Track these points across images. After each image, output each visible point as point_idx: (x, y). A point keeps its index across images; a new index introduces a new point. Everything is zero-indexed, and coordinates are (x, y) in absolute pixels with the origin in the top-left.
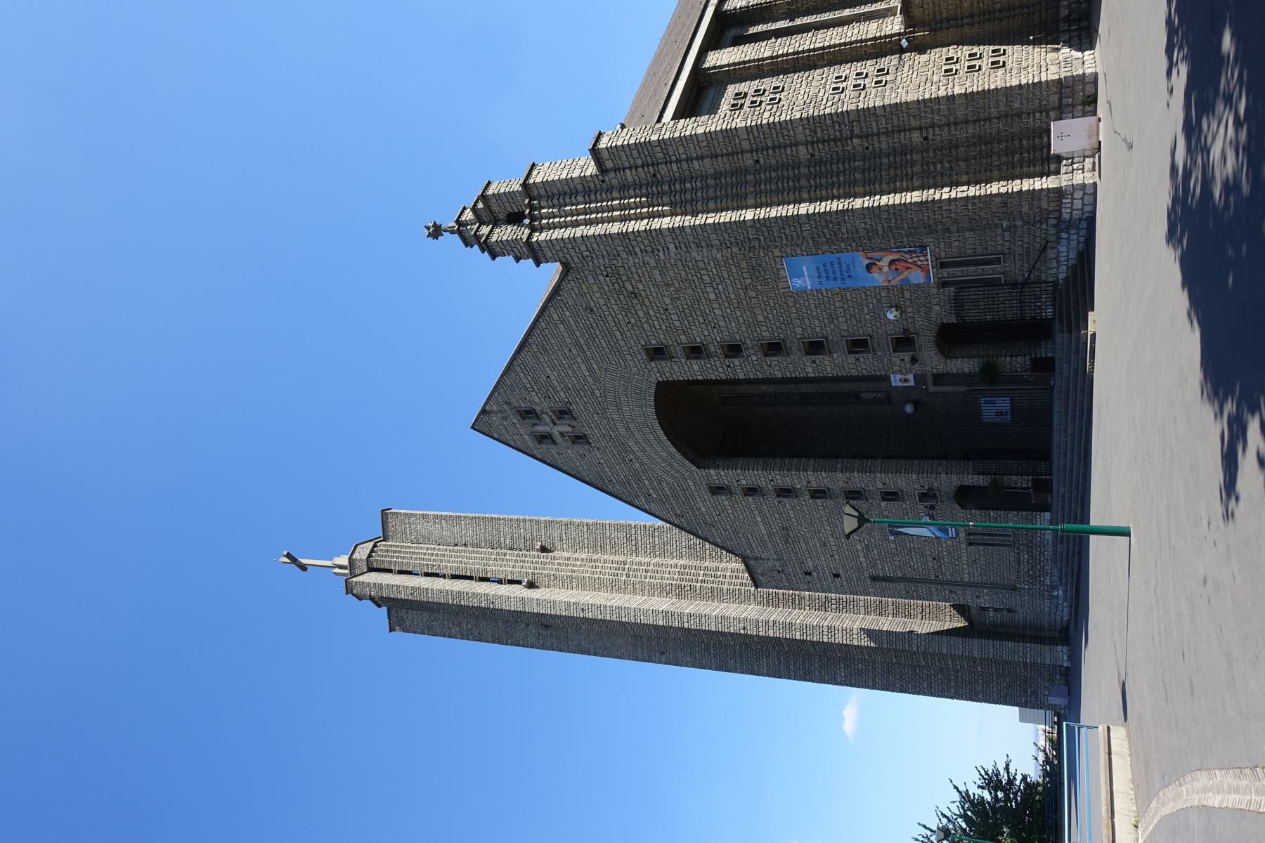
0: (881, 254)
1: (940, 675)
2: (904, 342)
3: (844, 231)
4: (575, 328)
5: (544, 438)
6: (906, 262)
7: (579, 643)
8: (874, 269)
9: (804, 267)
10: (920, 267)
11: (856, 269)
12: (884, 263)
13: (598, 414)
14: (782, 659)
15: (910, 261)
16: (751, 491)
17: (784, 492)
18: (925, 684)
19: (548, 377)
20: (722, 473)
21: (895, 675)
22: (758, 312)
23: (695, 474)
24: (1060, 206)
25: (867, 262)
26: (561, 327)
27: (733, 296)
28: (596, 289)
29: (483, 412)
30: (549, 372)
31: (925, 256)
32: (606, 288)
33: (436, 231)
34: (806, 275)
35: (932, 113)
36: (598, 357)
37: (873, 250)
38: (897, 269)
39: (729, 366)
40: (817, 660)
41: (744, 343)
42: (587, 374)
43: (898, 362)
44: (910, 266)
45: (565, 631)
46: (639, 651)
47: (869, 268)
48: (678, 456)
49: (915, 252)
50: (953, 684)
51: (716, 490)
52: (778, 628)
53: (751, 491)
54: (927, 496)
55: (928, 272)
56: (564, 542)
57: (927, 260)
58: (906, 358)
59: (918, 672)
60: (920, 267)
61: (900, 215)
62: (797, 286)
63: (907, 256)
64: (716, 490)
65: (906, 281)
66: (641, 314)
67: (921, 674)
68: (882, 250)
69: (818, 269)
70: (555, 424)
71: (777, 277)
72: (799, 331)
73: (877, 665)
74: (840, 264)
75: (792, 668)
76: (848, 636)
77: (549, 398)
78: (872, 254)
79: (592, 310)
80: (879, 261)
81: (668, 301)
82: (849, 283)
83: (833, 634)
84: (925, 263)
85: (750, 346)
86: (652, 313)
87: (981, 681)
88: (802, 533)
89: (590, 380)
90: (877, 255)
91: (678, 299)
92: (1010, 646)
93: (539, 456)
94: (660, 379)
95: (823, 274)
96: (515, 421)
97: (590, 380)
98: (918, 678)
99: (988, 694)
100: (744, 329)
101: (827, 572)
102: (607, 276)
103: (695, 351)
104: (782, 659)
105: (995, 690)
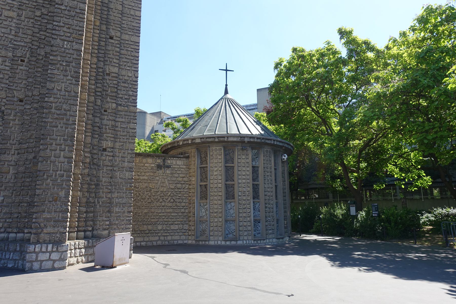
24: (45, 242)
35: (122, 157)
61: (63, 119)
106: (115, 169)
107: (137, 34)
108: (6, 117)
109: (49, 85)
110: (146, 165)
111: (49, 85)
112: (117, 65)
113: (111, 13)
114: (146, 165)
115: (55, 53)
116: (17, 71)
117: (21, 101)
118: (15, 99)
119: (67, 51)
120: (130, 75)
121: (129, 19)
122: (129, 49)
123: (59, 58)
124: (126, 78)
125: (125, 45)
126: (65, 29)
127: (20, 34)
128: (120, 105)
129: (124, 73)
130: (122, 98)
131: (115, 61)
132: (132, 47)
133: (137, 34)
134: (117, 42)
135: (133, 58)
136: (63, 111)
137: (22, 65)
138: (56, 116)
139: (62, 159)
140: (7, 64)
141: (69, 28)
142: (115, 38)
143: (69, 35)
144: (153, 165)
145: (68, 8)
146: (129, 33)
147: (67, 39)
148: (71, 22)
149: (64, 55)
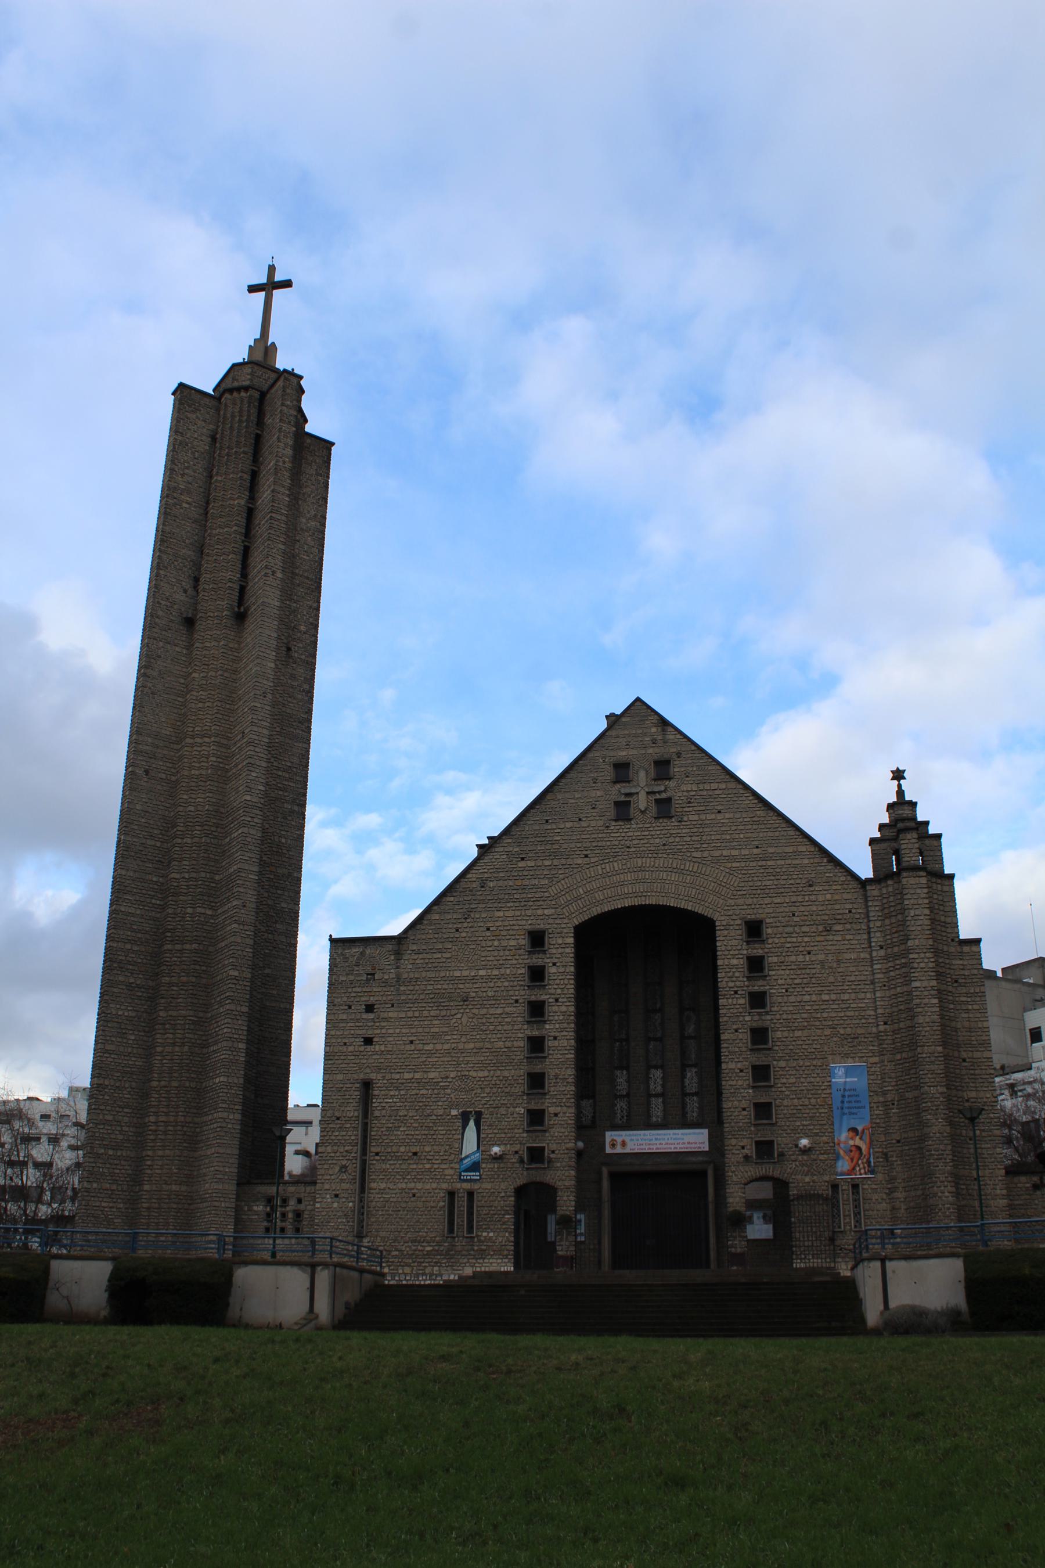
0: (868, 1140)
1: (121, 1137)
2: (765, 1149)
3: (929, 1117)
4: (787, 862)
5: (622, 771)
6: (859, 1159)
7: (160, 657)
8: (851, 1134)
9: (856, 1079)
10: (854, 1169)
11: (853, 1120)
12: (857, 1141)
13: (664, 845)
14: (140, 935)
15: (860, 1162)
16: (537, 975)
17: (537, 1010)
18: (110, 1118)
19: (719, 812)
20: (568, 950)
21: (120, 1080)
22: (806, 1033)
23: (566, 921)
25: (860, 1128)
26: (790, 849)
27: (825, 1015)
28: (836, 897)
29: (664, 723)
30: (727, 816)
31: (866, 1173)
32: (837, 907)
33: (898, 775)
34: (848, 1080)
35: (994, 1185)
36: (750, 872)
37: (871, 1135)
38: (851, 1151)
39: (736, 992)
40: (138, 982)
41: (767, 1013)
42: (725, 853)
43: (742, 1144)
44: (855, 1161)
45: (176, 641)
46: (150, 740)
47: (854, 1130)
48: (596, 911)
49: (869, 1166)
50: (111, 1152)
51: (537, 940)
52: (243, 949)
53: (537, 975)
54: (536, 1155)
55: (848, 1175)
56: (289, 681)
57: (861, 1174)
58: (746, 1151)
59: (126, 1110)
60: (854, 1169)
61: (941, 1159)
62: (836, 1071)
63: (865, 1160)
64: (537, 940)
65: (838, 1157)
66: (805, 929)
67: (122, 1114)
68: (871, 1141)
69: (854, 1090)
70: (648, 793)
71: (846, 1056)
72: (782, 1064)
73: (133, 1059)
74: (858, 1108)
75: (128, 946)
76: (235, 1036)
77: (689, 802)
78: (868, 1134)
79: (811, 886)
80: (861, 1138)
81: (821, 957)
82: (837, 1113)
83: (238, 1017)
84: (858, 1173)
85: (763, 1018)
86: (806, 939)
87: (114, 1187)
88: (459, 1016)
89: (717, 853)
90: (866, 1137)
91: (823, 968)
92: (229, 1227)
93: (590, 755)
94: (717, 923)
95: (847, 1093)
96: (650, 751)
97: (717, 853)
98: (117, 1109)
99: (99, 1195)
100: (785, 1016)
101: (378, 1031)
102: (850, 912)
103: (756, 965)
104: (140, 935)
105: (104, 1204)
106: (988, 1197)
107: (988, 1049)
108: (890, 1159)
109: (927, 1130)
110: (1019, 1185)
111: (927, 1130)
112: (974, 1089)
113: (960, 1034)
114: (1019, 1185)
115: (925, 1100)
116: (891, 1115)
117: (898, 1141)
118: (894, 1141)
119: (935, 1096)
120: (988, 1096)
121: (978, 1033)
122: (983, 1067)
123: (929, 1104)
124: (985, 1100)
125: (979, 1064)
126: (929, 1076)
127: (887, 1080)
128: (984, 1131)
129: (982, 1094)
130: (983, 1123)
131: (971, 1084)
132: (986, 1064)
133: (988, 1049)
134: (970, 1064)
135: (988, 1077)
136: (940, 1152)
137: (893, 1109)
138: (936, 1157)
139: (947, 1194)
140: (881, 1109)
141: (932, 1074)
142: (968, 1060)
143: (933, 1080)
144: (1028, 1185)
145: (928, 1055)
146: (980, 1049)
147: (933, 1084)
148: (932, 1067)
149: (933, 1099)
